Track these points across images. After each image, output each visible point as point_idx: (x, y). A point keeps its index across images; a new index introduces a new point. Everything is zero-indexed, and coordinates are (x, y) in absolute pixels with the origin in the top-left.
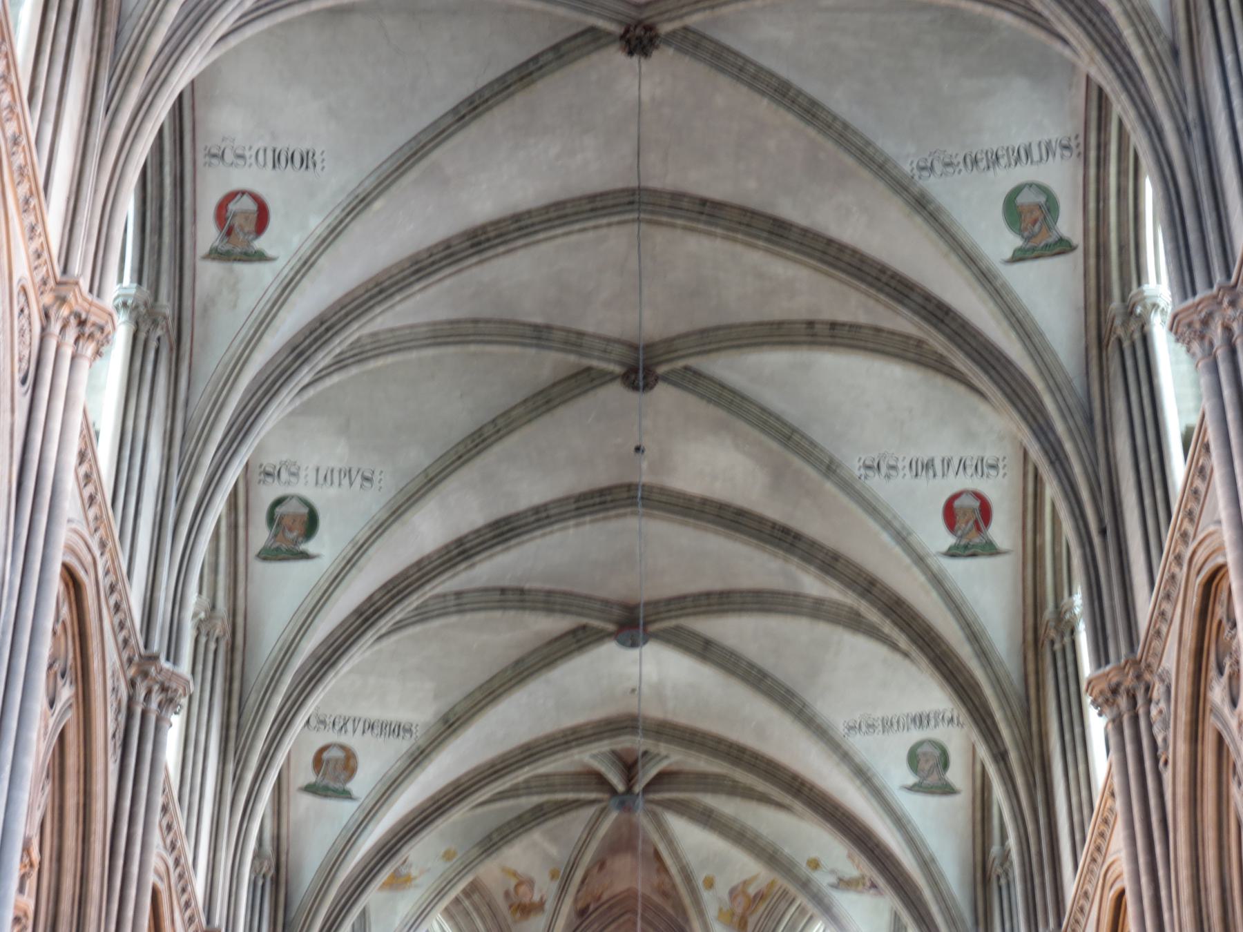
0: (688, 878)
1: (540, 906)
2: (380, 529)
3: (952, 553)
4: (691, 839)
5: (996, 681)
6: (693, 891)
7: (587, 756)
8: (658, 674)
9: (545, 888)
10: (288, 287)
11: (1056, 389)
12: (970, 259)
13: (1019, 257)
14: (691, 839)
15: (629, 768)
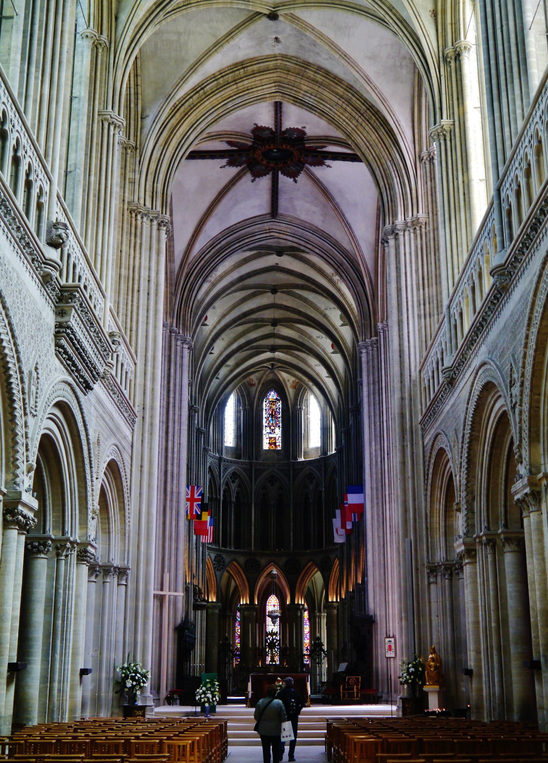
0: (284, 380)
1: (254, 385)
2: (226, 349)
3: (333, 353)
4: (284, 376)
5: (340, 378)
6: (285, 383)
7: (265, 365)
8: (278, 355)
9: (255, 381)
10: (211, 331)
11: (348, 351)
12: (333, 326)
13: (342, 325)
14: (284, 375)
15: (273, 365)
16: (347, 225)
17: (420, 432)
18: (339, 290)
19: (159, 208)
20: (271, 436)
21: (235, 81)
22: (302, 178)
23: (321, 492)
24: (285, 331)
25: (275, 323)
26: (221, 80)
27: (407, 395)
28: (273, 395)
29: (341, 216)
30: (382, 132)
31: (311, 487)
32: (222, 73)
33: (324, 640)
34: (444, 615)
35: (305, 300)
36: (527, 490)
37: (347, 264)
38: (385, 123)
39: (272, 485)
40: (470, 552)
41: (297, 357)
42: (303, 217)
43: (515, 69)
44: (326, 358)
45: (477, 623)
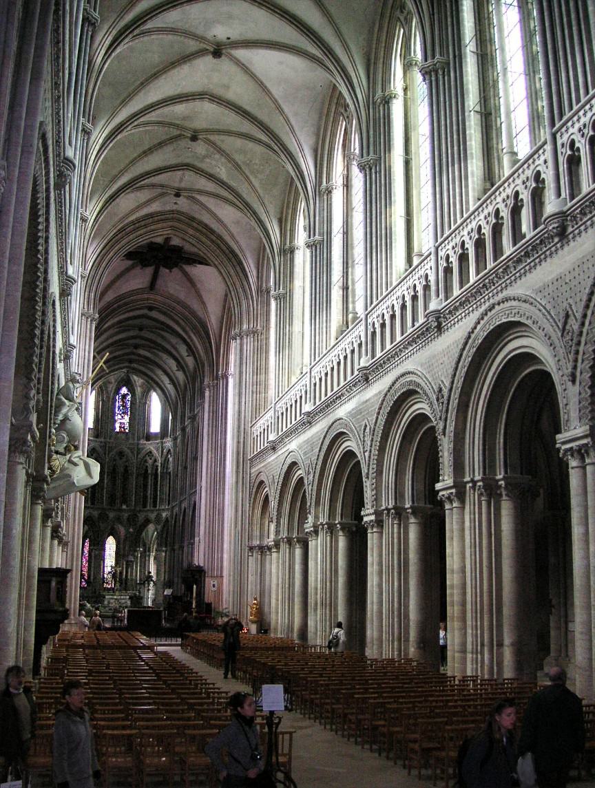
8: (135, 365)
9: (113, 381)
12: (181, 356)
14: (135, 377)
16: (203, 303)
17: (248, 465)
18: (190, 337)
19: (91, 311)
20: (122, 421)
21: (145, 226)
22: (175, 270)
23: (157, 466)
24: (142, 352)
25: (136, 347)
26: (137, 225)
27: (242, 440)
28: (124, 390)
29: (200, 296)
30: (238, 268)
31: (150, 461)
32: (138, 220)
33: (153, 573)
34: (256, 574)
35: (163, 337)
36: (312, 529)
37: (201, 328)
38: (240, 263)
39: (121, 459)
40: (277, 545)
41: (149, 369)
42: (172, 292)
43: (325, 305)
44: (172, 374)
45: (278, 585)
